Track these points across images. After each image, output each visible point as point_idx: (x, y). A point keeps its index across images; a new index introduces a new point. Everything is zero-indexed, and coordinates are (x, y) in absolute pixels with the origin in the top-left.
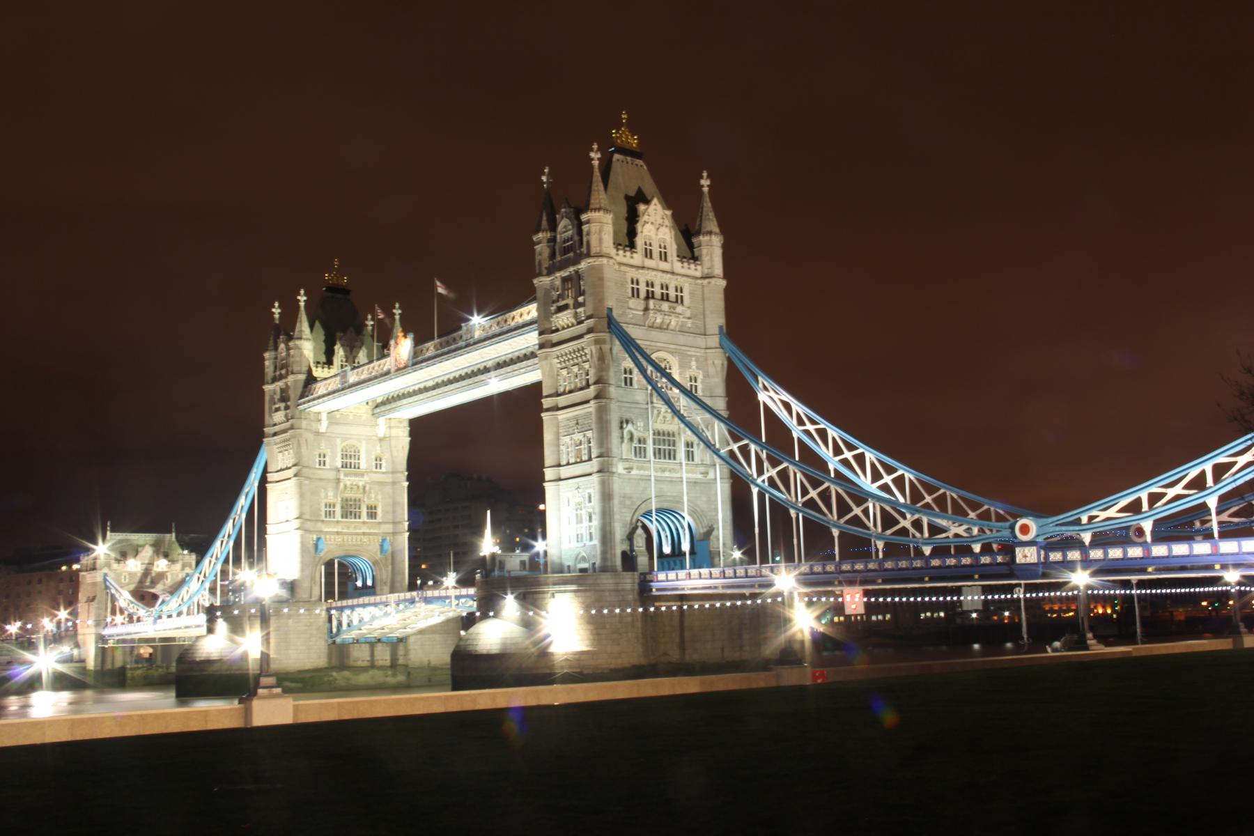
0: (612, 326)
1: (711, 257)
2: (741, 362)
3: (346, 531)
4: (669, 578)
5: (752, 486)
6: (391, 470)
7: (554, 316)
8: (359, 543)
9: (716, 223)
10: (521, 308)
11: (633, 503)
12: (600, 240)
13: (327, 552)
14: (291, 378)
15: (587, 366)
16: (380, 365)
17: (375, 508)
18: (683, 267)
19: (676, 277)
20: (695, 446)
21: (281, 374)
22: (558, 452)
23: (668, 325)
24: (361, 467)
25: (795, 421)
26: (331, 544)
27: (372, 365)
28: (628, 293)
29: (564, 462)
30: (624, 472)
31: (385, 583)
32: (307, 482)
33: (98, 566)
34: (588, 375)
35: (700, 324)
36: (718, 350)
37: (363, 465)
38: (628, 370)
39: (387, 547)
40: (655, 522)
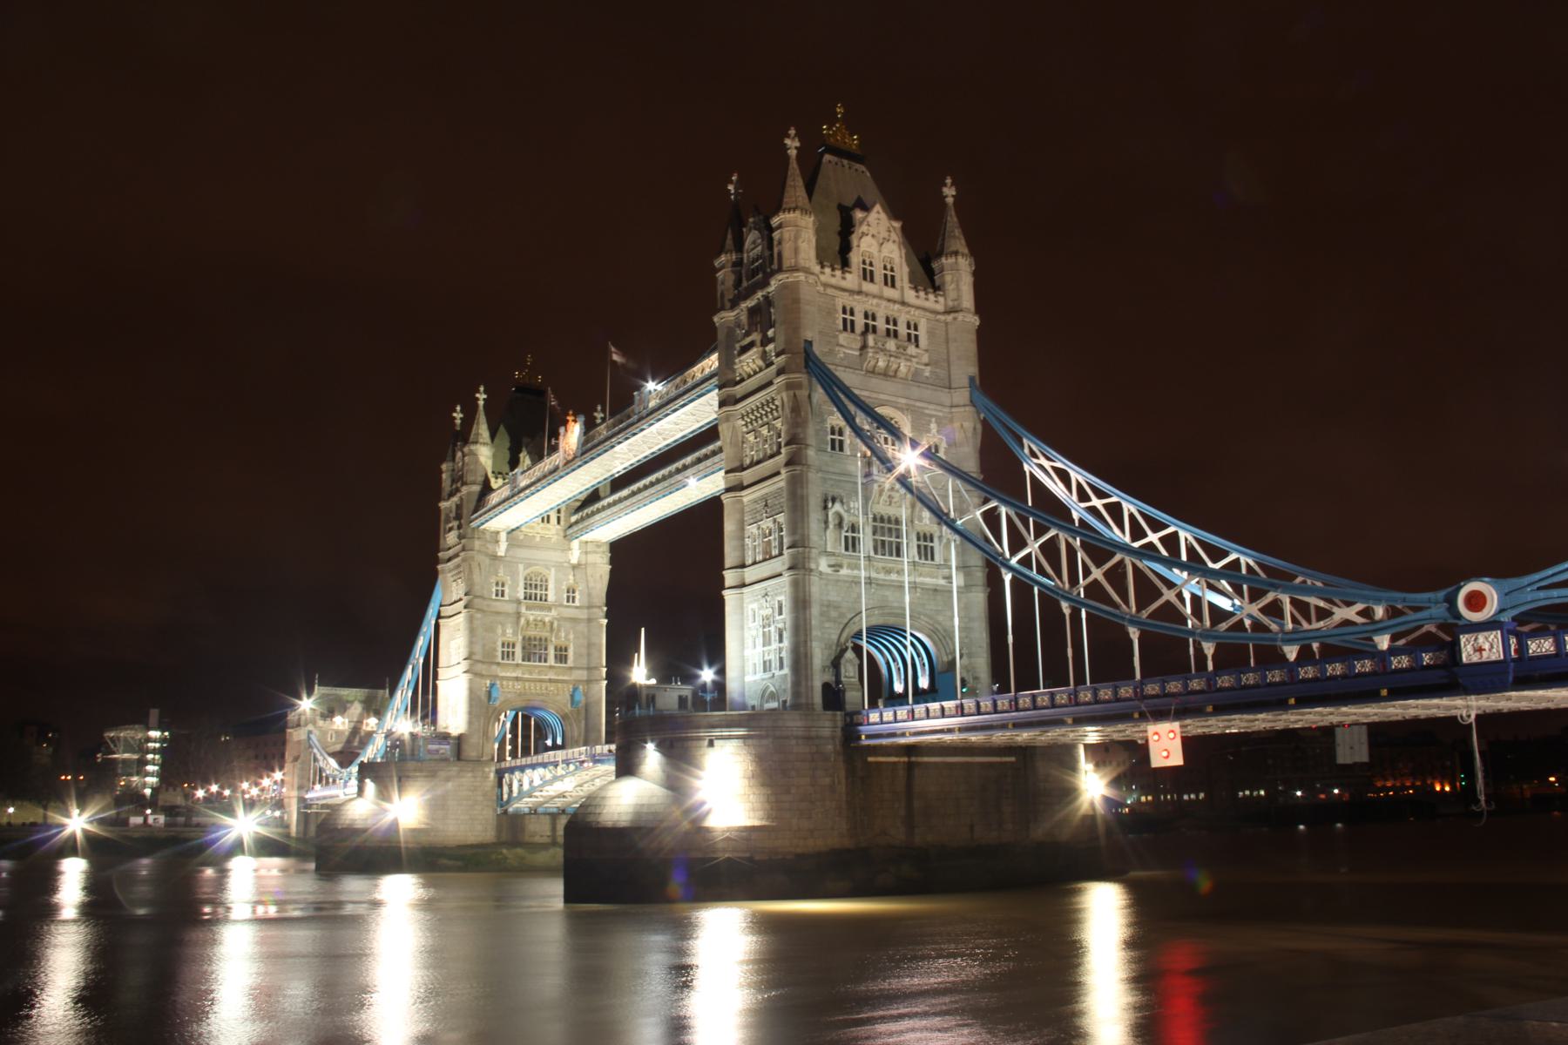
0: (811, 363)
1: (958, 285)
2: (997, 418)
3: (526, 676)
4: (885, 719)
5: (1003, 571)
6: (586, 604)
8: (545, 691)
9: (963, 242)
10: (700, 362)
11: (842, 615)
12: (796, 251)
13: (505, 701)
14: (465, 490)
17: (566, 650)
19: (908, 309)
20: (936, 540)
22: (743, 547)
23: (896, 371)
24: (549, 599)
25: (1075, 497)
27: (543, 464)
28: (838, 325)
29: (749, 561)
30: (829, 570)
32: (479, 615)
33: (302, 723)
34: (780, 437)
35: (942, 373)
36: (967, 409)
37: (551, 597)
38: (837, 429)
39: (579, 697)
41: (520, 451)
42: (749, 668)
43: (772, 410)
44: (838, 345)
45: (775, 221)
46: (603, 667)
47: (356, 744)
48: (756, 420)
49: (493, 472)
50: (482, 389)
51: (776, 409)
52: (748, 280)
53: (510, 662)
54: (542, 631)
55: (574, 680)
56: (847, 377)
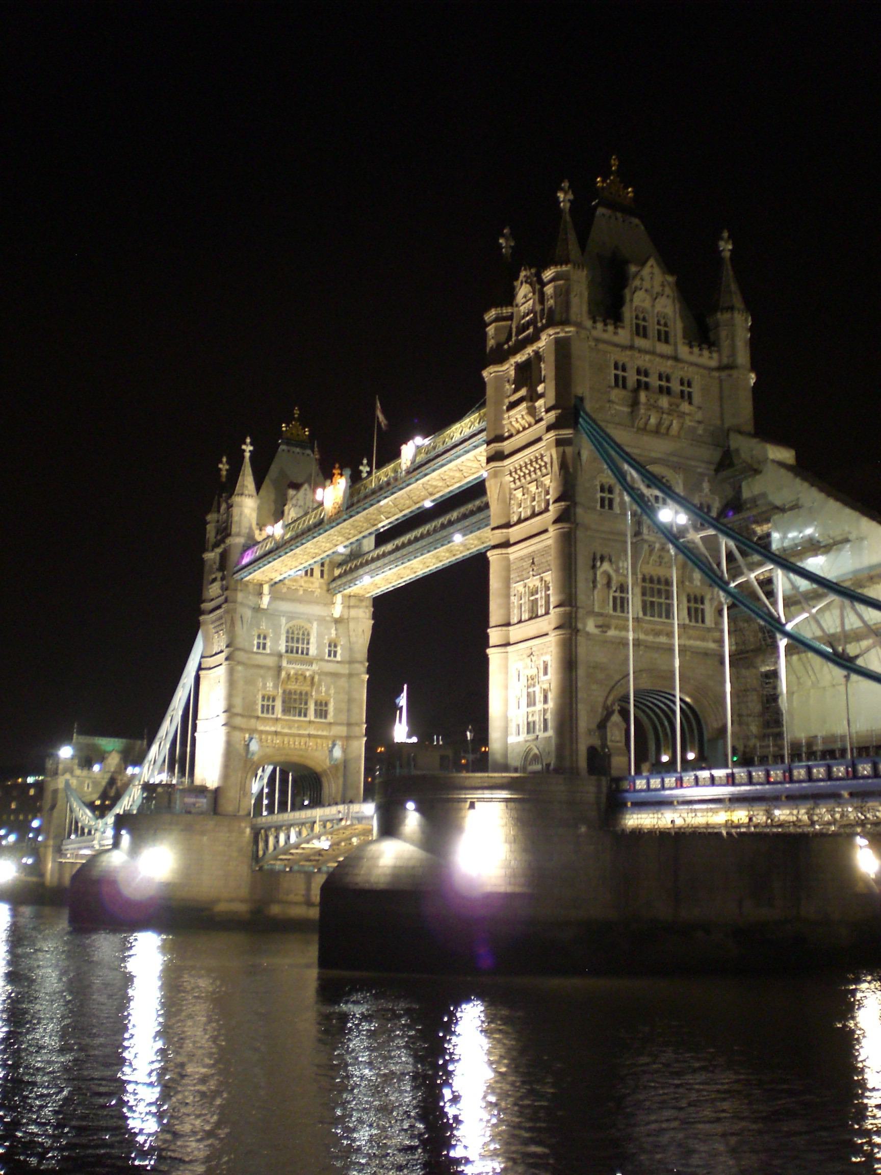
0: (581, 420)
1: (733, 340)
3: (286, 731)
4: (652, 786)
5: (778, 636)
6: (347, 658)
8: (303, 747)
17: (326, 705)
18: (691, 353)
19: (680, 365)
20: (707, 602)
29: (515, 620)
32: (240, 668)
33: (60, 771)
37: (313, 651)
38: (606, 487)
42: (512, 729)
43: (541, 466)
44: (610, 401)
45: (548, 274)
48: (524, 476)
49: (258, 524)
50: (248, 440)
51: (545, 466)
53: (270, 716)
54: (301, 686)
56: (621, 436)
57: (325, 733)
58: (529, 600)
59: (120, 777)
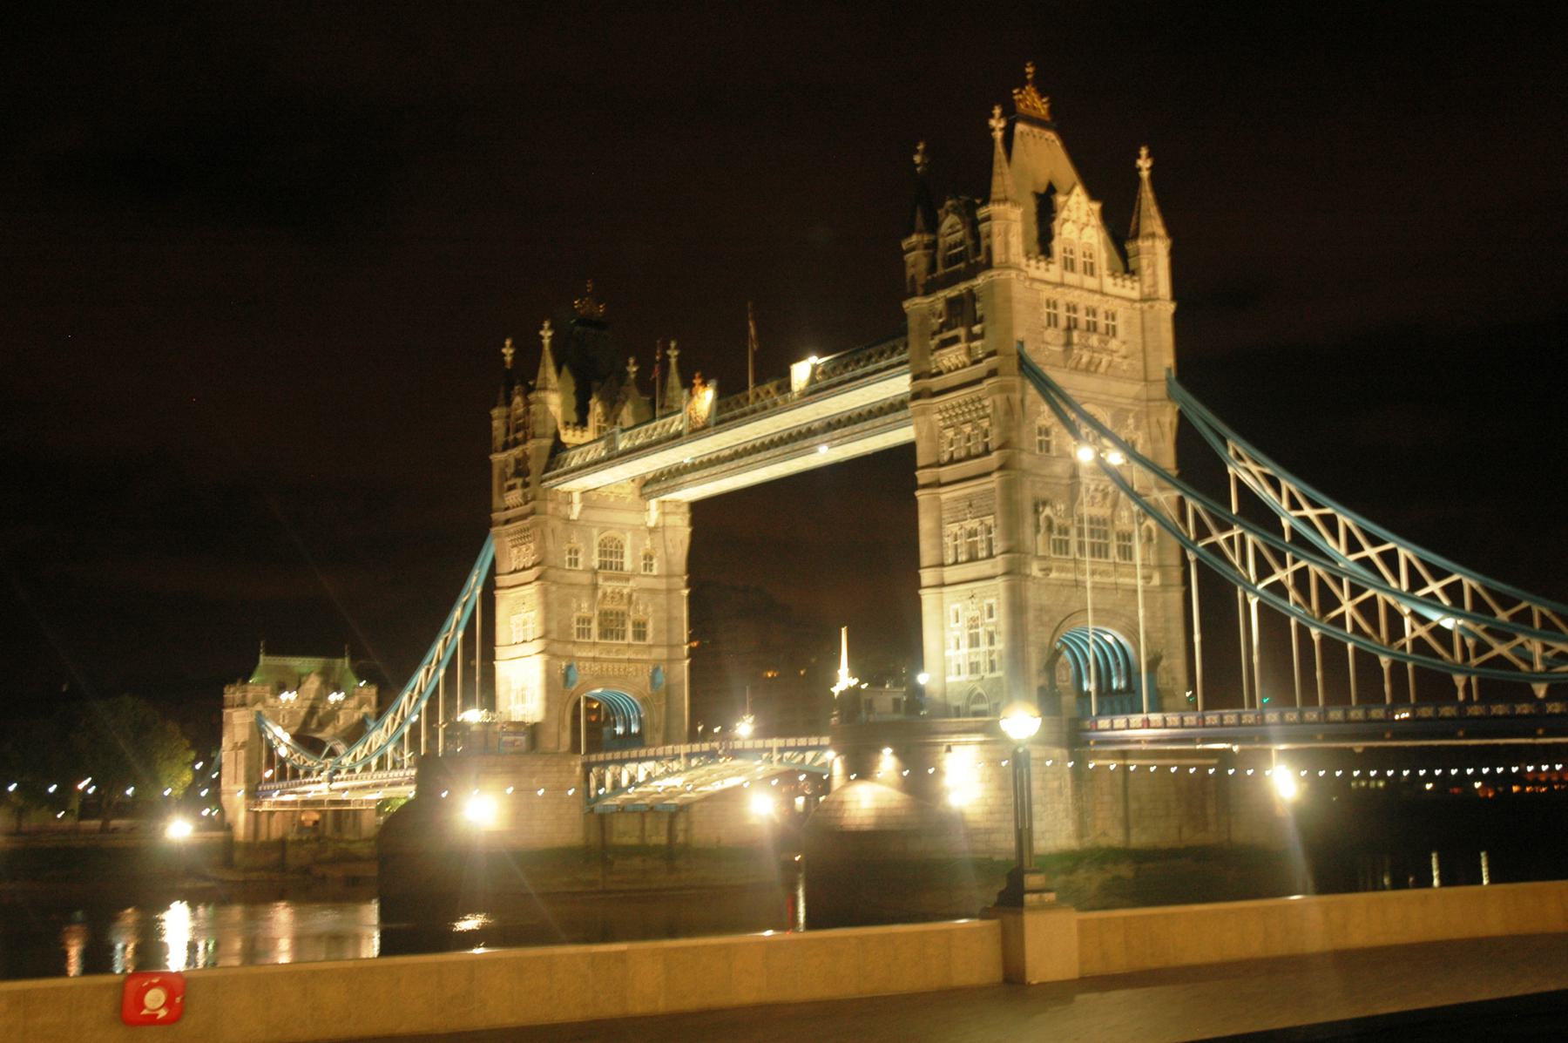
0: (1024, 367)
3: (604, 656)
4: (1116, 726)
6: (664, 572)
7: (937, 353)
12: (1007, 245)
13: (582, 684)
14: (531, 445)
15: (985, 423)
16: (664, 425)
17: (644, 625)
18: (1115, 285)
19: (1106, 299)
21: (515, 439)
22: (941, 546)
25: (1285, 505)
26: (585, 675)
27: (653, 425)
29: (950, 560)
30: (1040, 574)
31: (657, 730)
32: (554, 588)
35: (1139, 365)
37: (628, 566)
39: (660, 678)
40: (1092, 646)
41: (590, 398)
44: (1044, 342)
45: (982, 213)
46: (684, 644)
47: (313, 726)
52: (946, 267)
53: (586, 640)
55: (656, 660)
56: (1058, 376)
57: (645, 657)
58: (966, 542)
59: (321, 706)
